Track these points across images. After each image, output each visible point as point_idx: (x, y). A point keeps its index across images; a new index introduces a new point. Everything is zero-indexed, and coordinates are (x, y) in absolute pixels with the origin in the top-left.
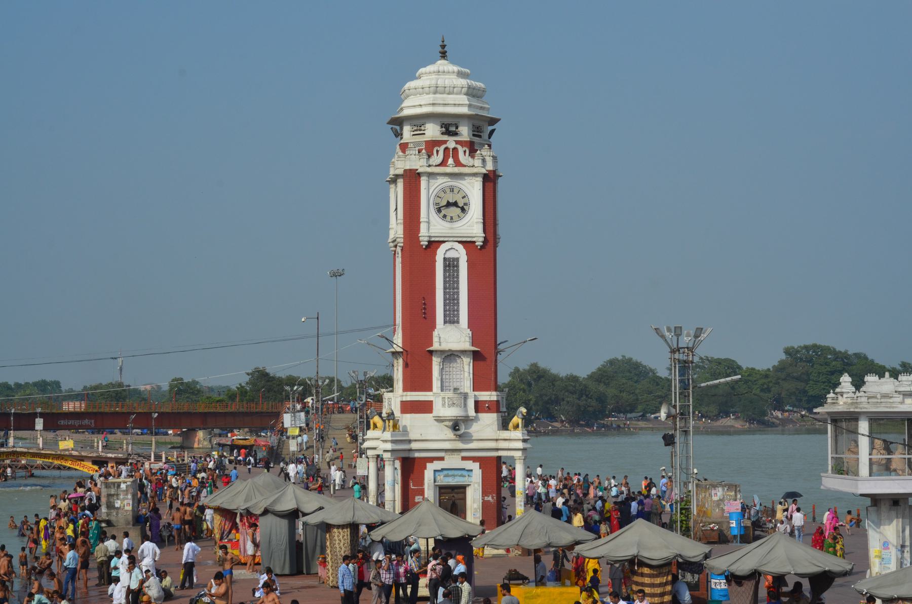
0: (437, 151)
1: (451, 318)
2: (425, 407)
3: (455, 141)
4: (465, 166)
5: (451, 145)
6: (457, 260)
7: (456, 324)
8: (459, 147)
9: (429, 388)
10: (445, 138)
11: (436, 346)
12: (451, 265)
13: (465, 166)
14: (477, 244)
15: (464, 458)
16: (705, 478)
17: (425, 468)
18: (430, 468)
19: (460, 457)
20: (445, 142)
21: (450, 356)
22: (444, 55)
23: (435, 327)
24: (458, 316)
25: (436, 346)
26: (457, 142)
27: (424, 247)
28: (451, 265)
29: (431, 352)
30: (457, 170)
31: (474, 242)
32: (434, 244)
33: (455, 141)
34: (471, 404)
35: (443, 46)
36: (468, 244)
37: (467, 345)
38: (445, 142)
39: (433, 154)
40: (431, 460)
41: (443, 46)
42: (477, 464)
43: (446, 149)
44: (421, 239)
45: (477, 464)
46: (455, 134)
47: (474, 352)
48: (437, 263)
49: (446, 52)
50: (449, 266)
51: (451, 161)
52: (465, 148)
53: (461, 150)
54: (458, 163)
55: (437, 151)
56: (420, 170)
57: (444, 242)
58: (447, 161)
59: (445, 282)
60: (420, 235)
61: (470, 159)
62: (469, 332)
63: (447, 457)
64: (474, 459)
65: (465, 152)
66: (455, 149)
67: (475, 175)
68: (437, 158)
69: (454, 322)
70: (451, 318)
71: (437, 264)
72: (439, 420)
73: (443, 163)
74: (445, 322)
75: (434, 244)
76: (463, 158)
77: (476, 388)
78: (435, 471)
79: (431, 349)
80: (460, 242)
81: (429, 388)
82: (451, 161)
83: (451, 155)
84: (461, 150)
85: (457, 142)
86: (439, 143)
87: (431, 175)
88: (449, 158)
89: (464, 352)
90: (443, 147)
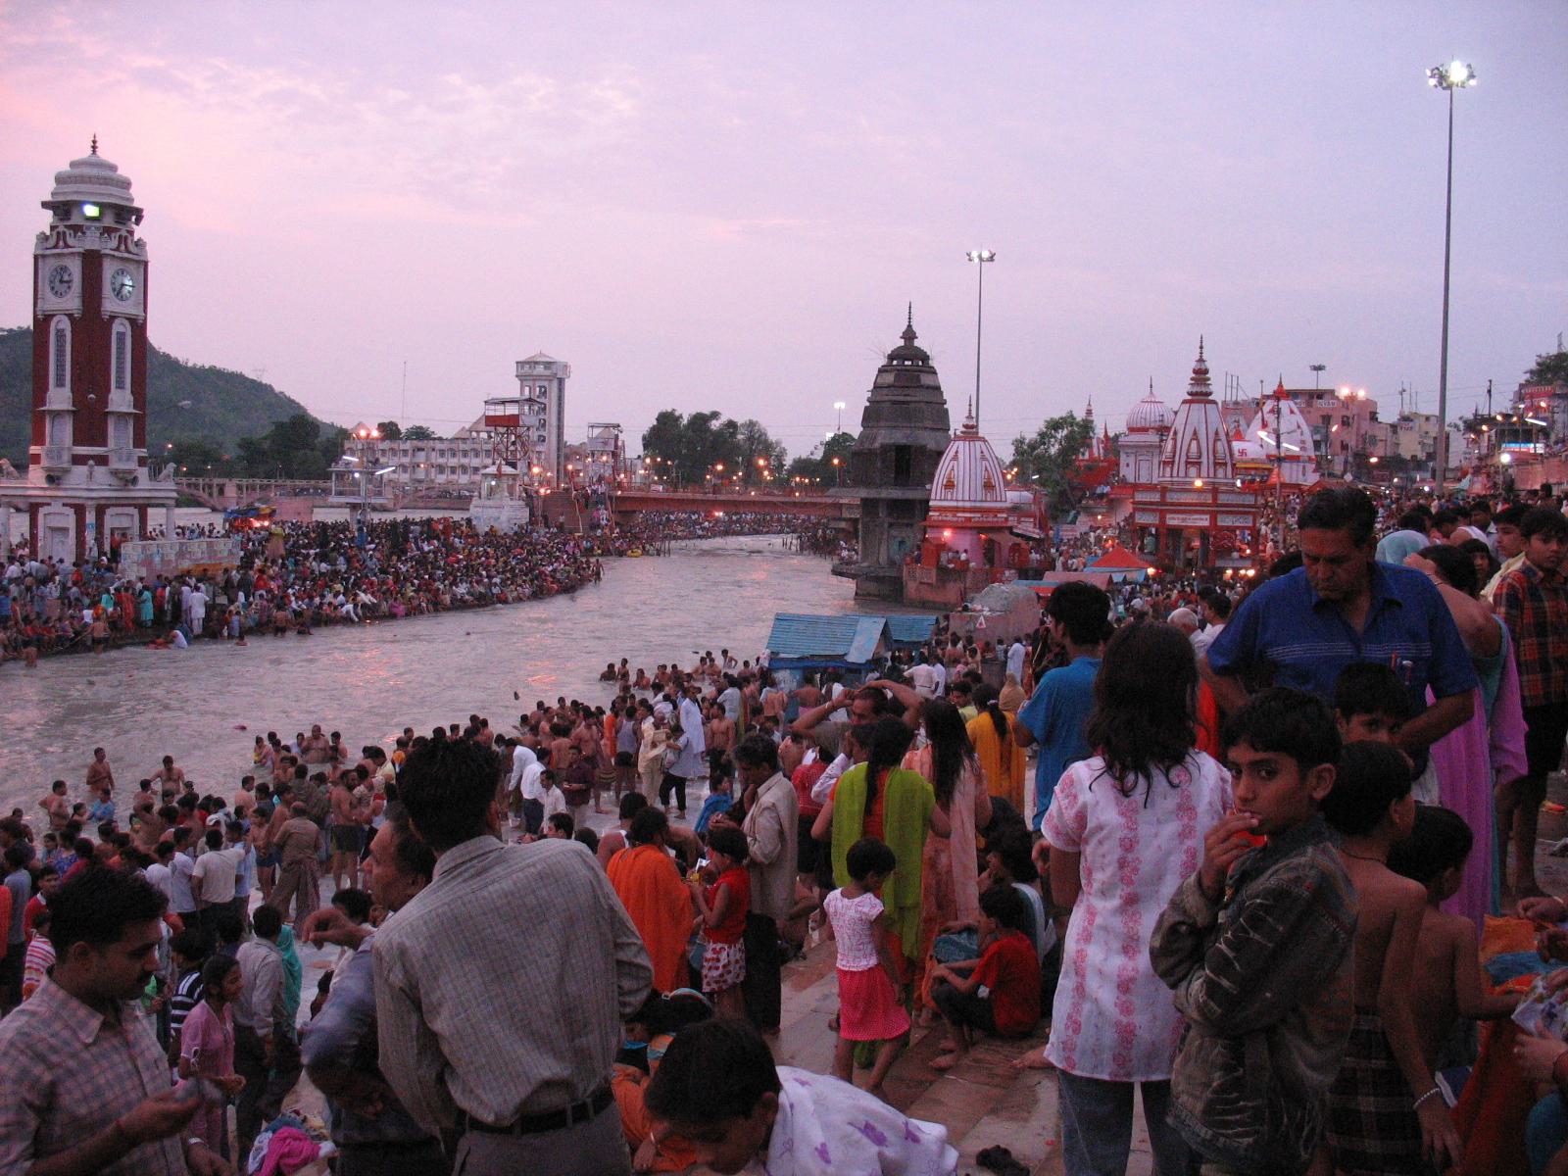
2: (102, 460)
9: (104, 444)
11: (111, 408)
15: (64, 505)
21: (121, 416)
25: (111, 408)
30: (126, 255)
32: (113, 318)
34: (66, 457)
40: (108, 506)
68: (114, 243)
72: (115, 473)
73: (117, 249)
75: (113, 318)
81: (104, 444)
89: (68, 411)
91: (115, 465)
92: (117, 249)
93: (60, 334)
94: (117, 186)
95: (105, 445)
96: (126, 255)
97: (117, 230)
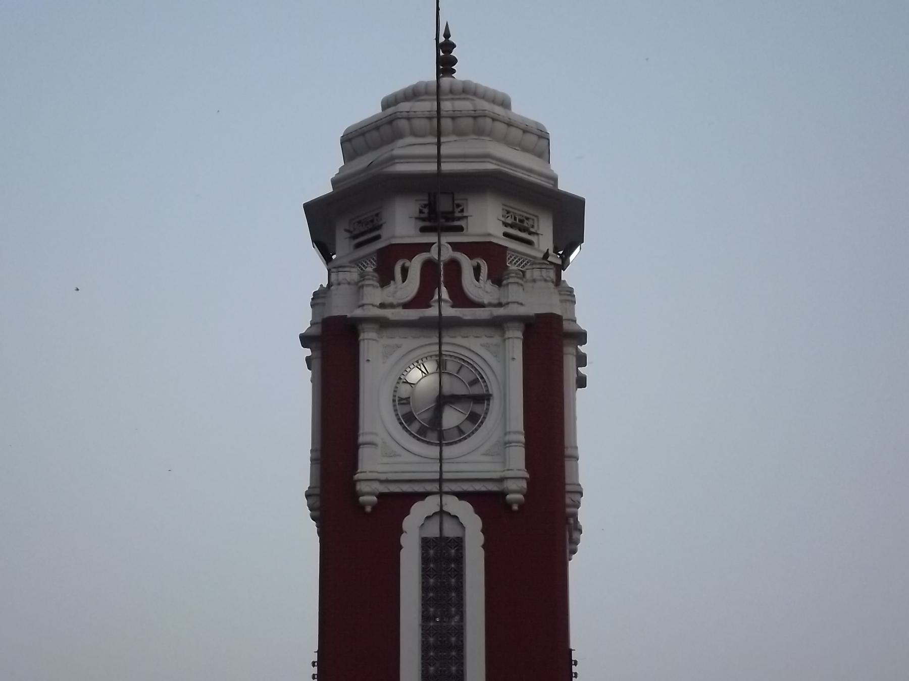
0: (405, 271)
3: (449, 243)
4: (481, 305)
6: (459, 543)
10: (431, 238)
13: (481, 305)
14: (508, 497)
20: (427, 247)
26: (456, 246)
27: (368, 509)
30: (449, 311)
31: (503, 494)
33: (449, 243)
39: (392, 278)
43: (429, 268)
44: (362, 487)
48: (402, 552)
49: (454, 61)
52: (475, 262)
53: (467, 264)
54: (460, 299)
56: (358, 313)
57: (422, 496)
60: (357, 477)
61: (489, 286)
65: (477, 270)
66: (454, 267)
71: (403, 554)
73: (421, 300)
80: (461, 495)
84: (467, 264)
85: (456, 246)
86: (411, 250)
87: (384, 324)
90: (423, 256)
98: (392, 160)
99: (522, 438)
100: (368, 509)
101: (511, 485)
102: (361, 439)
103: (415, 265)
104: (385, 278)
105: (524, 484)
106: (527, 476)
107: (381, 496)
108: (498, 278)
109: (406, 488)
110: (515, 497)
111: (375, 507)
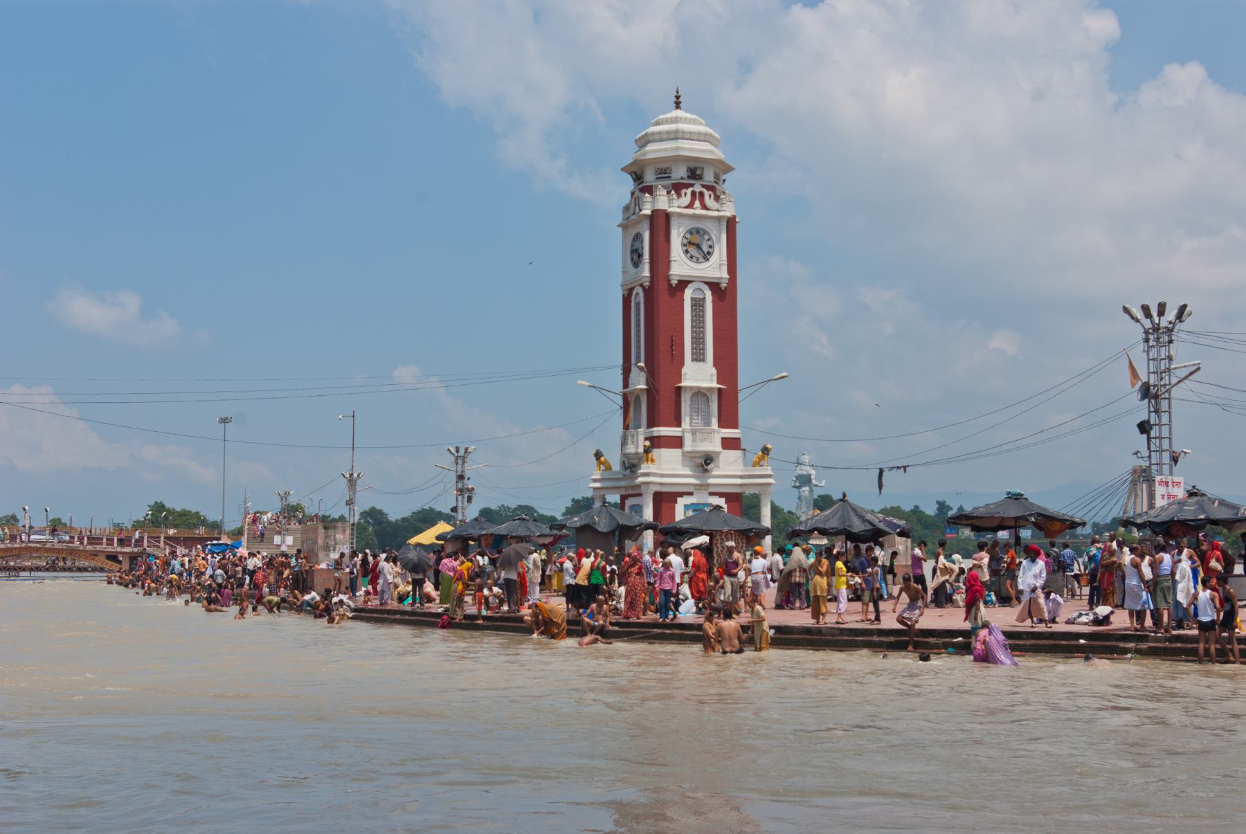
0: (685, 194)
1: (699, 356)
2: (677, 442)
5: (698, 189)
7: (701, 363)
8: (704, 190)
12: (698, 304)
16: (1134, 451)
17: (676, 502)
18: (681, 502)
19: (707, 492)
21: (700, 394)
22: (678, 105)
23: (683, 365)
24: (703, 354)
26: (703, 186)
27: (674, 286)
28: (698, 304)
29: (680, 388)
32: (683, 284)
33: (701, 185)
35: (678, 97)
36: (714, 286)
37: (715, 385)
38: (692, 185)
40: (682, 494)
41: (678, 97)
42: (723, 500)
43: (693, 193)
45: (723, 500)
46: (700, 177)
47: (720, 390)
49: (680, 102)
50: (695, 305)
51: (697, 203)
52: (710, 192)
53: (707, 193)
54: (704, 207)
55: (685, 194)
57: (692, 282)
58: (694, 204)
59: (692, 321)
61: (715, 203)
62: (714, 371)
63: (695, 492)
64: (721, 495)
65: (710, 196)
66: (701, 194)
67: (719, 218)
68: (686, 200)
69: (700, 361)
70: (699, 356)
73: (690, 206)
74: (693, 360)
75: (683, 284)
76: (710, 202)
77: (722, 424)
78: (685, 506)
79: (680, 385)
80: (706, 283)
82: (697, 203)
83: (697, 198)
84: (707, 193)
88: (696, 200)
90: (690, 189)
91: (688, 446)
92: (690, 206)
93: (638, 304)
94: (661, 140)
95: (679, 425)
96: (704, 212)
97: (688, 186)
98: (678, 149)
99: (726, 263)
100: (674, 286)
101: (723, 281)
102: (671, 259)
103: (689, 191)
104: (679, 196)
105: (727, 281)
106: (728, 277)
107: (678, 281)
108: (717, 198)
109: (688, 279)
110: (724, 285)
111: (676, 285)
